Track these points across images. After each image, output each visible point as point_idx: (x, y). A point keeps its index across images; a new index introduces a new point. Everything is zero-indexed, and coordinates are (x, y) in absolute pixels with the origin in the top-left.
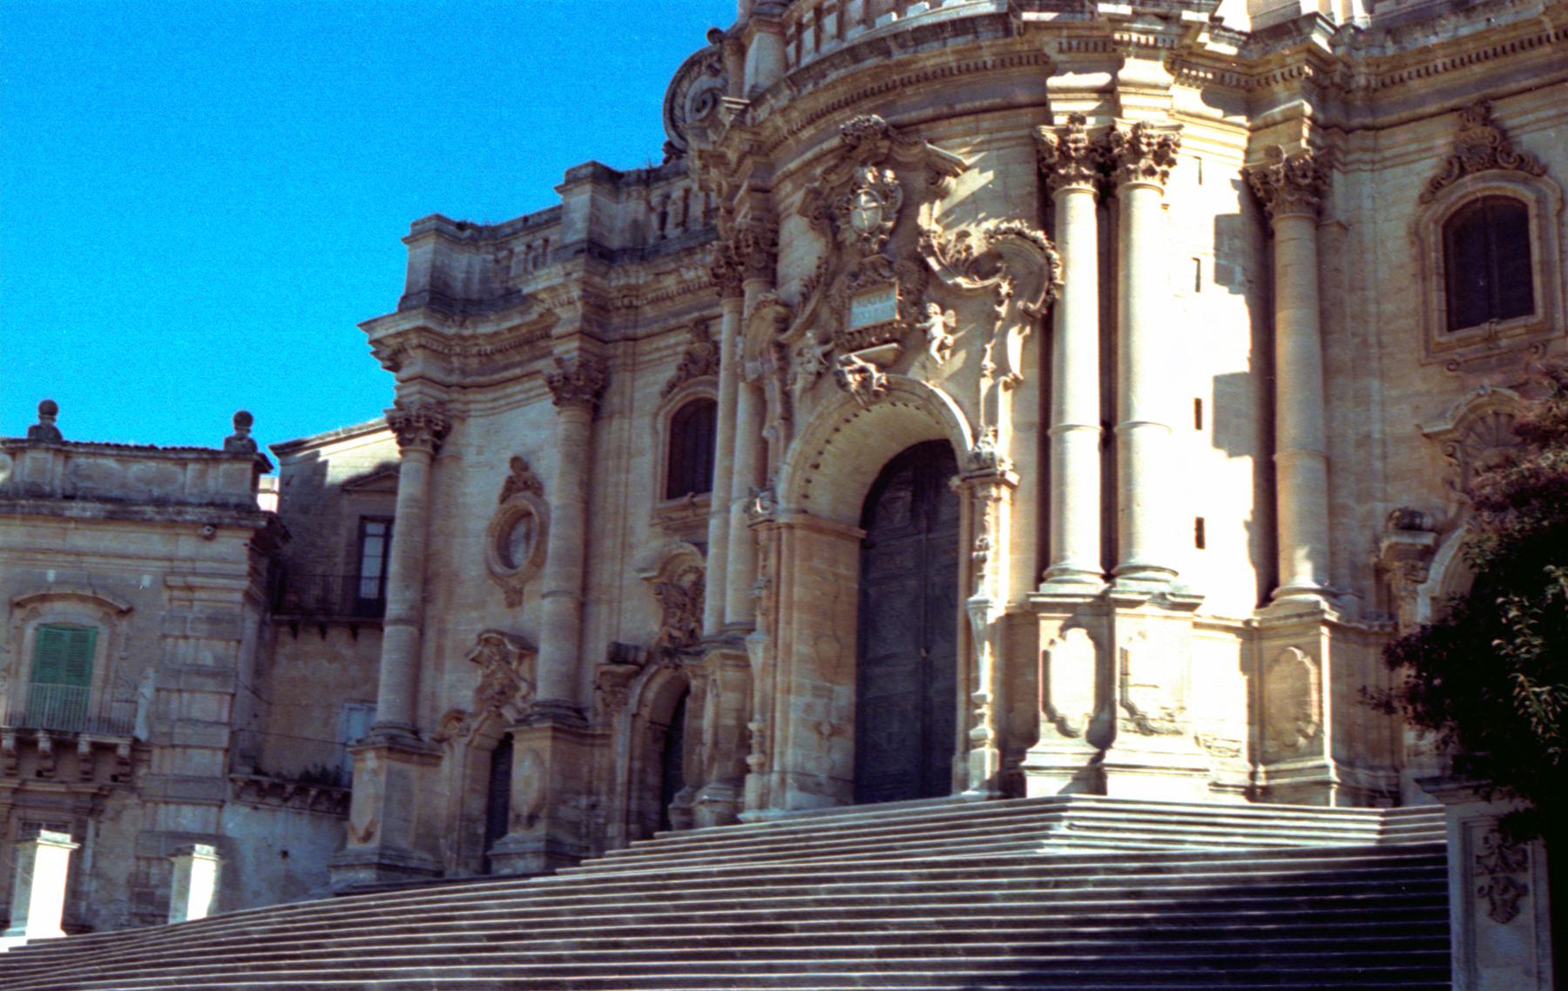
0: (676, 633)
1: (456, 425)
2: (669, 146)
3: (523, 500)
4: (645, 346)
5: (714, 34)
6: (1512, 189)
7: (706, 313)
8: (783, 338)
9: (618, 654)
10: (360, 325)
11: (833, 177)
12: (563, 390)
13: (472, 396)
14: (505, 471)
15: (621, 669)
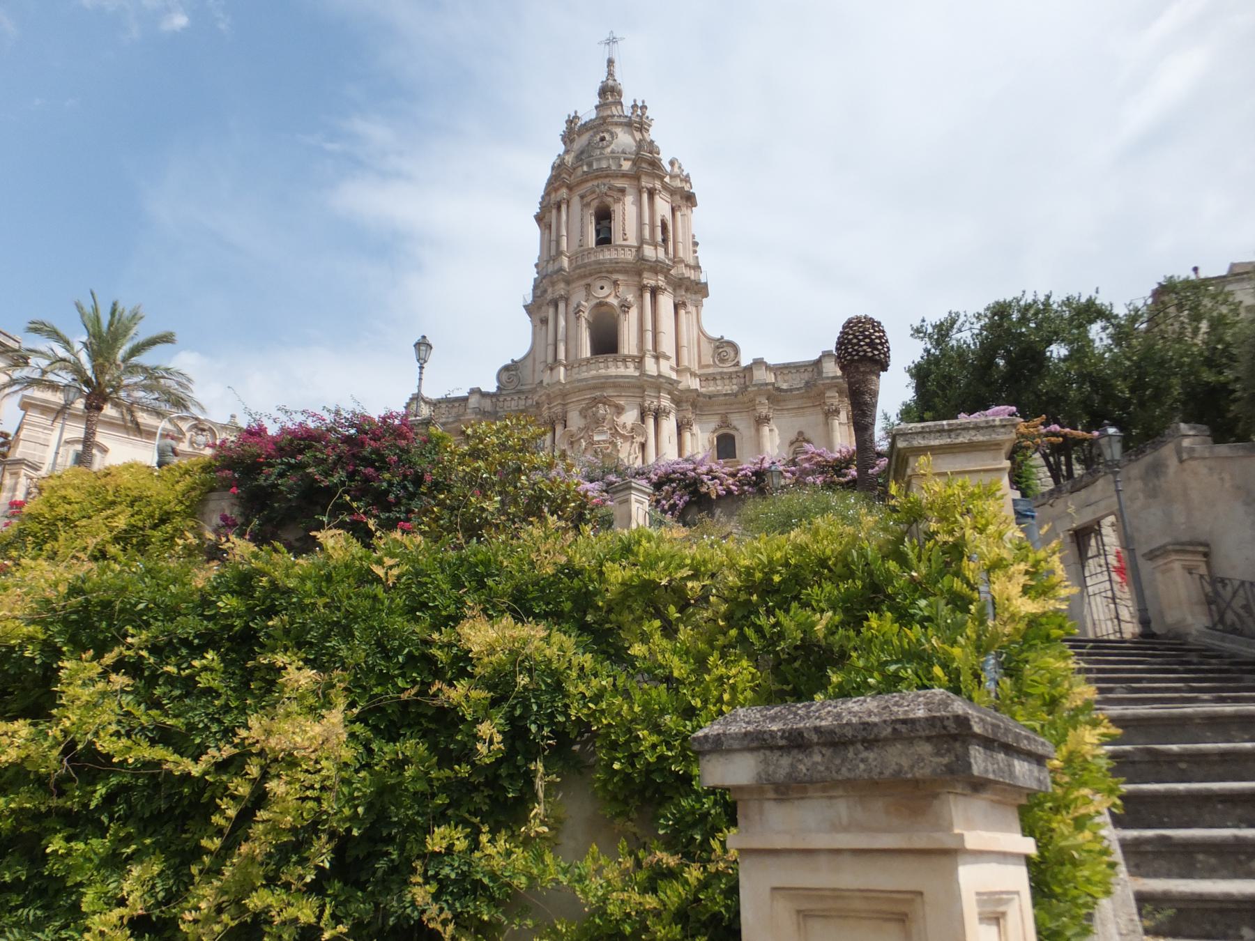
2: (498, 387)
5: (513, 360)
6: (732, 432)
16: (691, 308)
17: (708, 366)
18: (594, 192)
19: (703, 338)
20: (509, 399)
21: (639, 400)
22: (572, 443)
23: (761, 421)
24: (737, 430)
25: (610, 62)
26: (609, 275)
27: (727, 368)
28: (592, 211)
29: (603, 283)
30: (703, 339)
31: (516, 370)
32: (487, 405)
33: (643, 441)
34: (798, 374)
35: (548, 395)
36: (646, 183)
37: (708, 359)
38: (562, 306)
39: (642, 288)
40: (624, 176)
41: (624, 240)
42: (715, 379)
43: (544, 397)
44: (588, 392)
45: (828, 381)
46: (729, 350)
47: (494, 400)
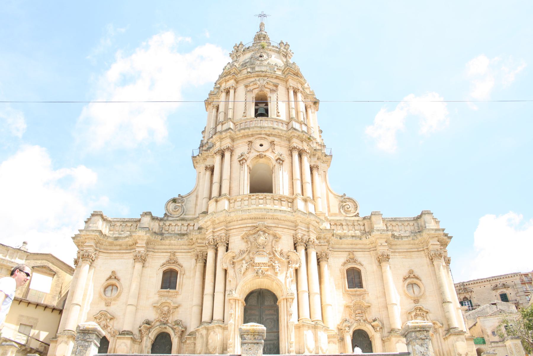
0: (162, 320)
1: (96, 260)
2: (166, 214)
3: (114, 281)
4: (157, 254)
6: (358, 267)
7: (175, 251)
8: (234, 260)
9: (148, 323)
10: (79, 230)
11: (251, 231)
12: (136, 259)
13: (101, 254)
14: (109, 274)
15: (148, 326)
16: (321, 172)
17: (335, 215)
18: (256, 84)
19: (330, 194)
20: (173, 224)
21: (293, 232)
22: (233, 263)
23: (382, 259)
24: (362, 265)
25: (262, 25)
26: (266, 137)
27: (351, 218)
28: (254, 95)
29: (262, 142)
30: (331, 196)
31: (183, 202)
32: (155, 226)
33: (297, 266)
34: (403, 227)
35: (213, 222)
36: (292, 83)
37: (335, 209)
38: (227, 155)
39: (291, 150)
40: (277, 78)
41: (278, 116)
42: (342, 225)
43: (209, 223)
44: (250, 221)
45: (433, 232)
46: (351, 204)
47: (161, 224)
